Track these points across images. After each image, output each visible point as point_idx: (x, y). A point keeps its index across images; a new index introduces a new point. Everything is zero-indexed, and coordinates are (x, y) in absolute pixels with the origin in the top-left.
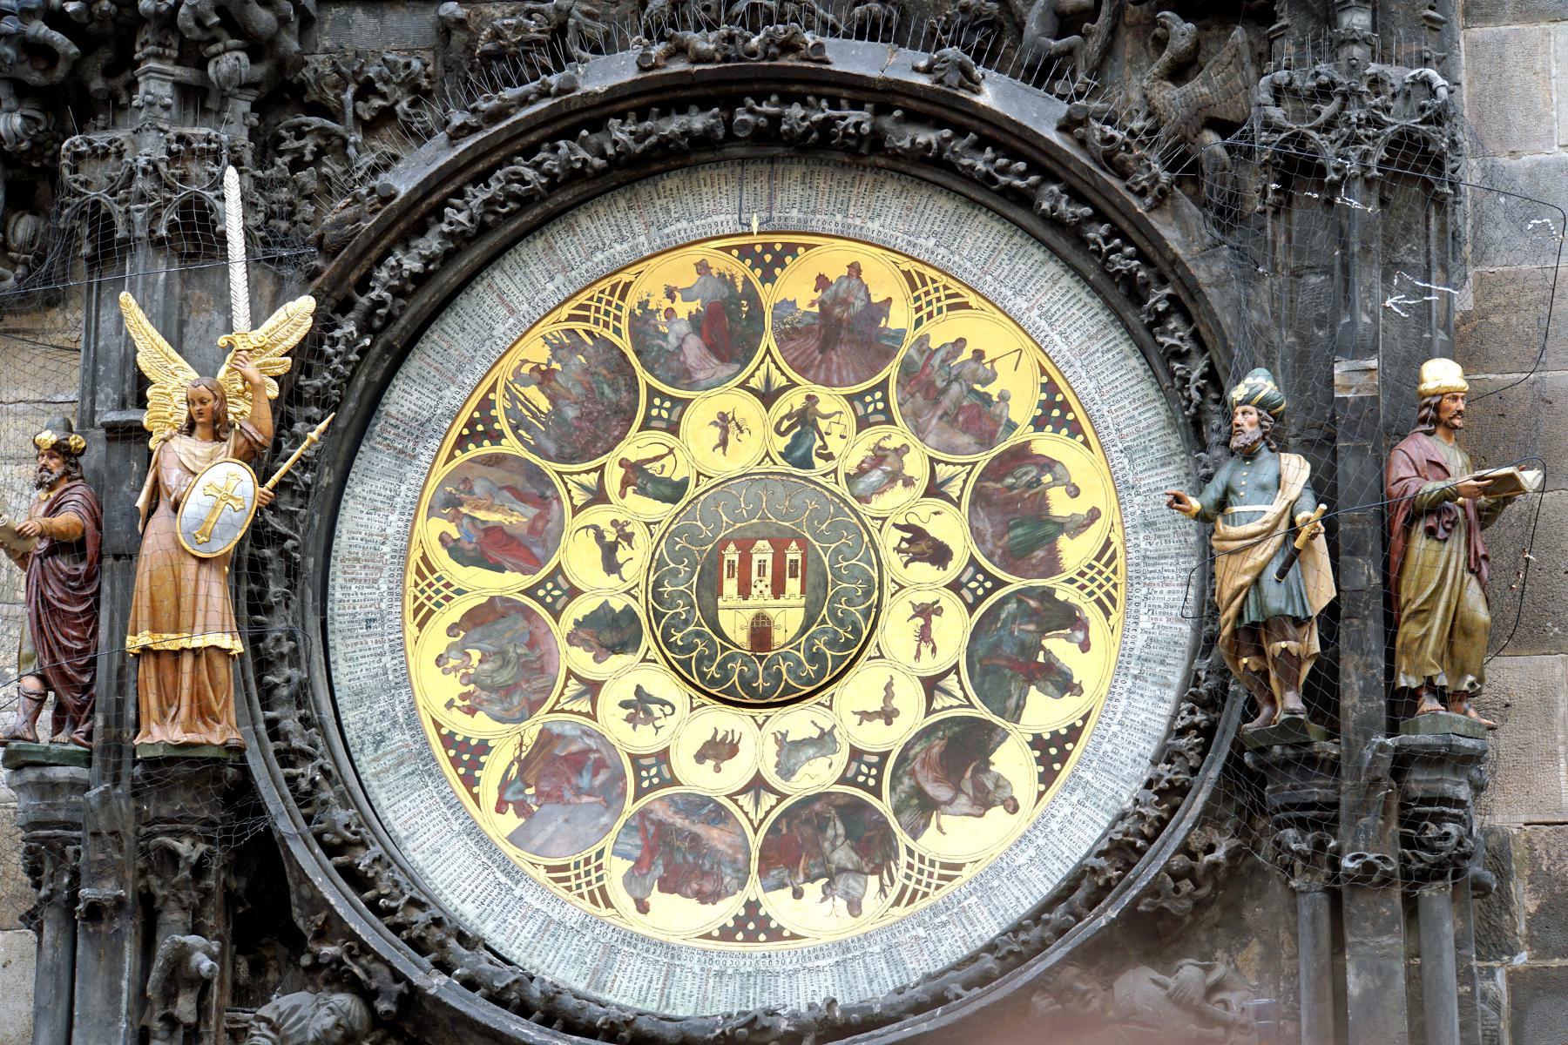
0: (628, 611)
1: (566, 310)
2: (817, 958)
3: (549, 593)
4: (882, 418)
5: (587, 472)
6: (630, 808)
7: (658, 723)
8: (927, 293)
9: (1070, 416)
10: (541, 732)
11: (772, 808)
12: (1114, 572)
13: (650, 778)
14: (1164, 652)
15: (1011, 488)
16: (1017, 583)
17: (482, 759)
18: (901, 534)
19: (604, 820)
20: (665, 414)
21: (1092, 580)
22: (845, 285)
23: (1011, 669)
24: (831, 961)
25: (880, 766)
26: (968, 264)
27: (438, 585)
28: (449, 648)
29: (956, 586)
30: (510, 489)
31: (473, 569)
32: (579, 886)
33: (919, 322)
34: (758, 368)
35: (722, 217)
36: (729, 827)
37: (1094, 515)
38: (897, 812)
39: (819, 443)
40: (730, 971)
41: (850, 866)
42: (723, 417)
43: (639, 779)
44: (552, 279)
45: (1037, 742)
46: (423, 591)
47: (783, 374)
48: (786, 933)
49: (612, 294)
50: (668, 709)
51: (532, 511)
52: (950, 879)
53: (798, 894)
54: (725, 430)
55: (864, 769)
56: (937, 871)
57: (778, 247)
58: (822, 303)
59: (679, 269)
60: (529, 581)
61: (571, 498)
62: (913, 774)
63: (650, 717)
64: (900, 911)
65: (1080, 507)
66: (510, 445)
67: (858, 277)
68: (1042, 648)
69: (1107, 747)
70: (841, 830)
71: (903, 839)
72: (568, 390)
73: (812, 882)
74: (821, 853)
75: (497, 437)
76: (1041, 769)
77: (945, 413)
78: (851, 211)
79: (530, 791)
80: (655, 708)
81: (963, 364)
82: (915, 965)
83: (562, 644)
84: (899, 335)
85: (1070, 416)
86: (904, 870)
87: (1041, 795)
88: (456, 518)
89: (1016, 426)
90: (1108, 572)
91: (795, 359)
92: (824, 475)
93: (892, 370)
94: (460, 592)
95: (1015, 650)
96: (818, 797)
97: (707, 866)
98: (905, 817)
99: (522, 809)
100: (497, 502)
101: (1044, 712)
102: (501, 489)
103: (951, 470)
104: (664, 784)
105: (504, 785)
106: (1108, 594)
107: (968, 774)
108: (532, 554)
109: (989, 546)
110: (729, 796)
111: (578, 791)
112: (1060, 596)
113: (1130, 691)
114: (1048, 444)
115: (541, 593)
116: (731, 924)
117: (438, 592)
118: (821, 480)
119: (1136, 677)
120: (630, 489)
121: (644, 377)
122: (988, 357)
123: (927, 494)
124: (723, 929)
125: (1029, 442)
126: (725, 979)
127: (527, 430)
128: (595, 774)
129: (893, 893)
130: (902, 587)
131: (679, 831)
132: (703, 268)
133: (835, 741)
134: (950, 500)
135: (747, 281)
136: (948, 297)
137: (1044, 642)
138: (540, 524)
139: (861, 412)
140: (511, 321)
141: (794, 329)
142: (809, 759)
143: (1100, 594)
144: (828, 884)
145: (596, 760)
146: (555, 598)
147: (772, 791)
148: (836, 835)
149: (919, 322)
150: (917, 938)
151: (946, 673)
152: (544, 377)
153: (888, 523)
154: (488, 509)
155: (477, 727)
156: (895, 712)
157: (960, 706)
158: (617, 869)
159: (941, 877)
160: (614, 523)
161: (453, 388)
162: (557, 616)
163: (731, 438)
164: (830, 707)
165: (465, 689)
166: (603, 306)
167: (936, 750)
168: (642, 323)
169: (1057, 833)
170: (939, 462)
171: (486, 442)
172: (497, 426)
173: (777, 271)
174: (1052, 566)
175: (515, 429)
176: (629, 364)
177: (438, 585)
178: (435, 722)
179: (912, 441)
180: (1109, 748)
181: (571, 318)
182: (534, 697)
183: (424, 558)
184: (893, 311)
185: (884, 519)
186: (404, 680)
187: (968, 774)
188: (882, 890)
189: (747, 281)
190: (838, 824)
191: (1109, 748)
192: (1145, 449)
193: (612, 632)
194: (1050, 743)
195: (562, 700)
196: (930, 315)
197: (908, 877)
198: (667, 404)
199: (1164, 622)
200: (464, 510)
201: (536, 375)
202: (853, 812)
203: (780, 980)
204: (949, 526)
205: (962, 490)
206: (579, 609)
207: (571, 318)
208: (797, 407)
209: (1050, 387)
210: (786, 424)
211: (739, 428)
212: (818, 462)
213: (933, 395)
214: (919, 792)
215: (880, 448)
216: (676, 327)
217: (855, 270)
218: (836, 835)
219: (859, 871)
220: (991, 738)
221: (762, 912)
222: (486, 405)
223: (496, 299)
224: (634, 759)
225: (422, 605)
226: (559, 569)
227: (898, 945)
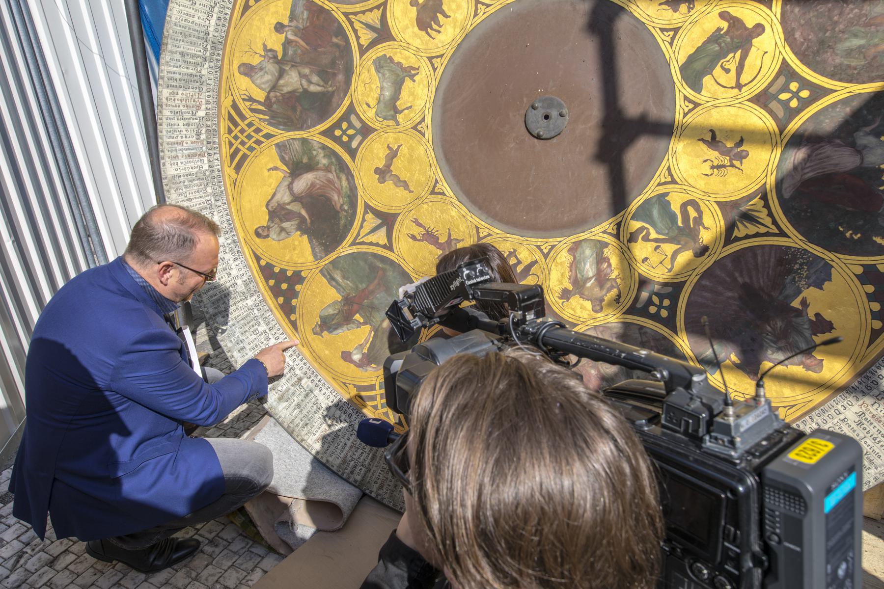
2: (219, 19)
11: (358, 38)
14: (305, 412)
23: (363, 290)
24: (211, 29)
25: (347, 147)
34: (770, 214)
38: (304, 141)
39: (653, 235)
41: (281, 82)
45: (297, 278)
47: (747, 237)
52: (233, 157)
53: (279, 28)
55: (351, 132)
56: (244, 150)
58: (799, 313)
62: (327, 169)
64: (227, 103)
68: (365, 323)
69: (262, 328)
70: (313, 88)
71: (283, 135)
73: (284, 45)
74: (304, 63)
82: (179, 96)
91: (755, 256)
95: (376, 302)
98: (297, 146)
101: (320, 295)
107: (304, 213)
119: (300, 379)
129: (243, 106)
137: (368, 328)
141: (790, 271)
142: (382, 88)
144: (275, 57)
147: (373, 44)
150: (199, 108)
153: (538, 256)
156: (382, 180)
157: (358, 234)
159: (237, 151)
164: (415, 128)
167: (336, 197)
185: (546, 256)
187: (304, 213)
188: (251, 99)
190: (319, 89)
194: (291, 288)
197: (250, 125)
198: (794, 104)
210: (693, 213)
211: (718, 167)
214: (310, 167)
218: (310, 82)
219: (274, 87)
220: (321, 244)
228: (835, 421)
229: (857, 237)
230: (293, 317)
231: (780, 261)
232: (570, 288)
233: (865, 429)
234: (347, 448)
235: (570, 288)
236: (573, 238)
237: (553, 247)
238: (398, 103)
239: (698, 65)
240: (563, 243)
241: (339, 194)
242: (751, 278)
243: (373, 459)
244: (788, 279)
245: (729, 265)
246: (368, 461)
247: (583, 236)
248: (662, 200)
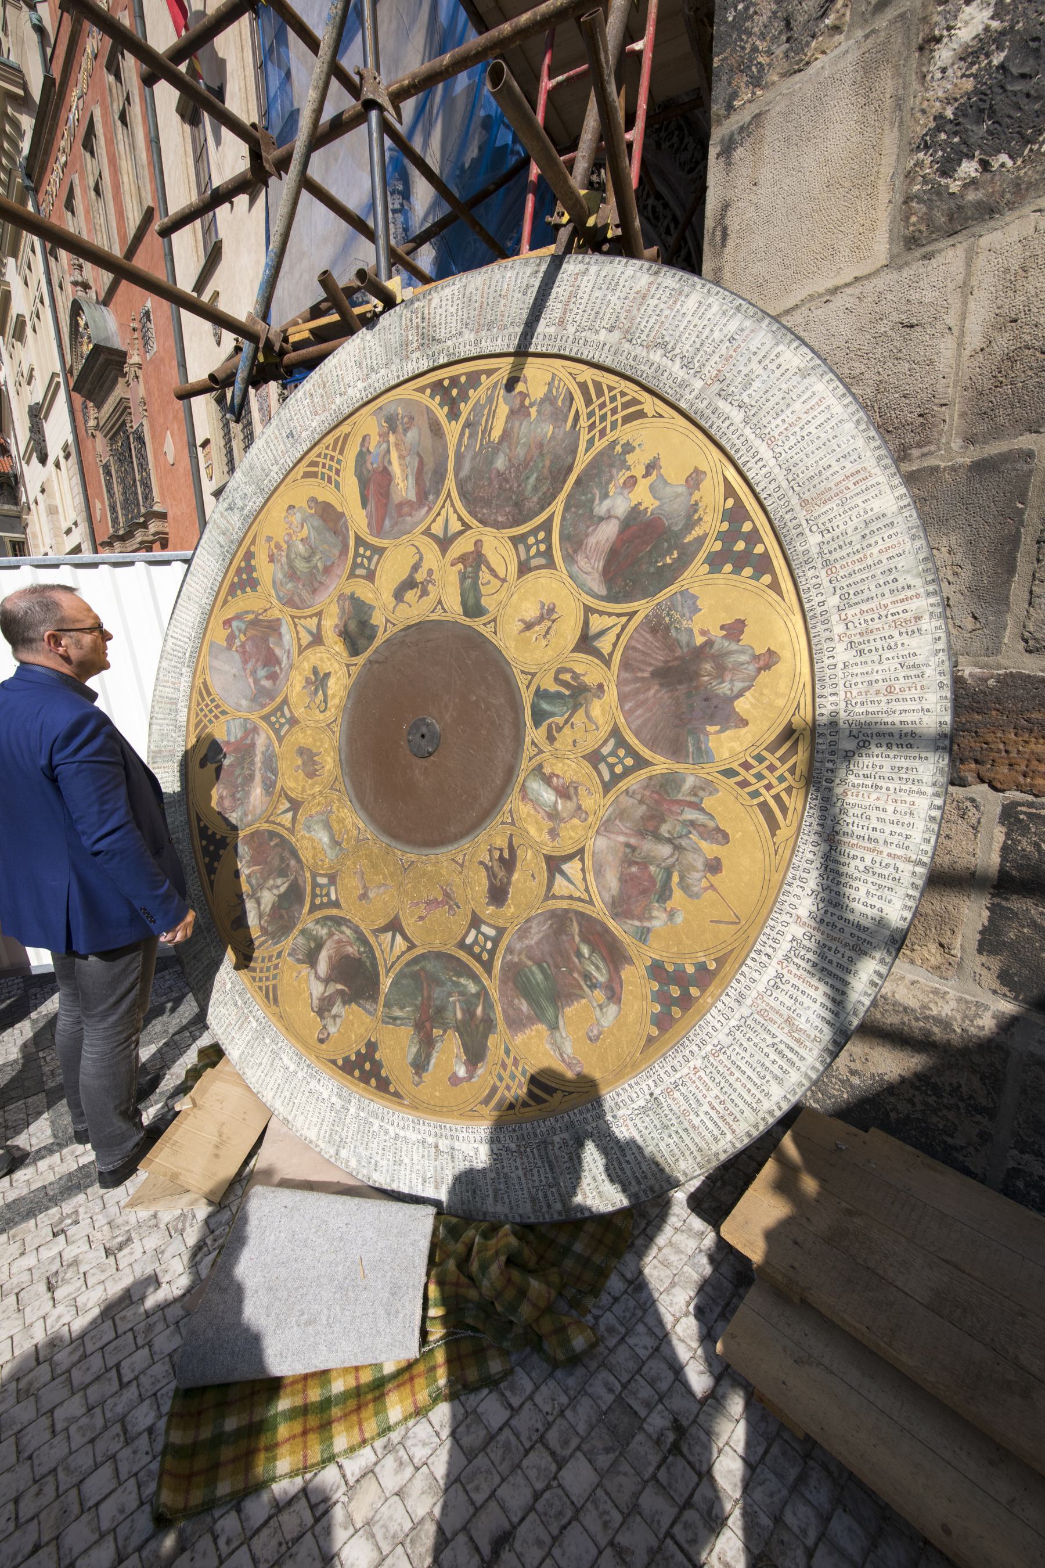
4: (607, 777)
6: (255, 717)
7: (312, 705)
8: (772, 768)
10: (279, 620)
15: (579, 954)
16: (493, 986)
18: (505, 845)
22: (744, 658)
23: (422, 1004)
29: (476, 922)
30: (421, 463)
32: (202, 710)
33: (729, 773)
39: (560, 720)
43: (273, 713)
45: (372, 1047)
47: (615, 645)
51: (412, 496)
52: (267, 997)
54: (541, 619)
56: (270, 983)
58: (709, 643)
62: (331, 935)
66: (452, 431)
67: (759, 670)
68: (445, 1032)
70: (282, 889)
72: (518, 443)
74: (266, 880)
75: (454, 415)
77: (634, 849)
78: (850, 612)
79: (243, 638)
81: (697, 850)
84: (703, 755)
88: (384, 436)
89: (644, 942)
91: (634, 649)
92: (533, 743)
95: (438, 1002)
96: (299, 861)
97: (238, 796)
98: (301, 940)
99: (231, 639)
100: (408, 459)
101: (397, 1048)
102: (418, 455)
105: (238, 617)
107: (339, 987)
108: (383, 520)
109: (518, 946)
110: (282, 789)
111: (254, 672)
112: (492, 1040)
119: (436, 1147)
120: (460, 566)
121: (558, 506)
122: (715, 879)
123: (549, 859)
124: (206, 828)
127: (469, 437)
128: (267, 678)
131: (252, 763)
132: (695, 479)
135: (700, 540)
138: (406, 509)
139: (605, 750)
141: (667, 628)
148: (278, 887)
149: (729, 773)
154: (401, 457)
155: (266, 571)
160: (430, 572)
162: (352, 575)
167: (350, 949)
170: (582, 860)
174: (516, 1024)
175: (468, 424)
176: (564, 481)
180: (376, 1128)
181: (583, 387)
182: (296, 599)
185: (513, 823)
187: (339, 987)
189: (700, 540)
191: (376, 1128)
192: (666, 1127)
196: (744, 784)
198: (543, 547)
200: (392, 438)
207: (583, 387)
210: (567, 677)
211: (547, 632)
213: (649, 826)
214: (319, 947)
215: (576, 788)
217: (768, 660)
218: (278, 887)
220: (367, 999)
224: (285, 701)
226: (380, 551)
228: (841, 675)
229: (675, 555)
231: (654, 631)
232: (551, 824)
233: (870, 651)
234: (523, 1181)
235: (551, 824)
236: (517, 788)
237: (510, 811)
239: (471, 601)
240: (513, 802)
241: (350, 944)
242: (651, 664)
243: (551, 1169)
244: (673, 633)
245: (627, 675)
246: (549, 1175)
247: (521, 779)
248: (541, 694)
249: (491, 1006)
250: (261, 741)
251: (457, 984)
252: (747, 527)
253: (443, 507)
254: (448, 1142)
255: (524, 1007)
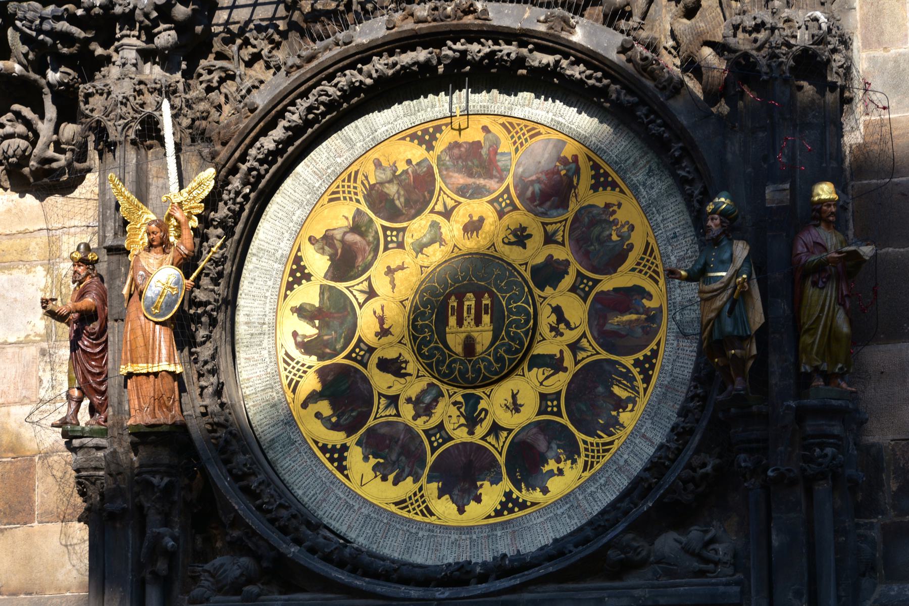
0: (542, 289)
1: (615, 447)
3: (586, 285)
5: (583, 359)
6: (509, 180)
9: (328, 455)
10: (568, 207)
11: (436, 204)
12: (287, 377)
13: (504, 200)
14: (252, 340)
15: (352, 411)
17: (593, 181)
19: (521, 170)
20: (549, 403)
21: (298, 370)
24: (379, 131)
26: (398, 526)
27: (645, 270)
28: (629, 236)
30: (623, 336)
31: (630, 285)
32: (521, 129)
33: (421, 489)
34: (504, 442)
35: (539, 521)
36: (455, 186)
37: (305, 405)
38: (371, 220)
39: (462, 410)
40: (429, 109)
41: (387, 185)
42: (517, 410)
44: (626, 461)
45: (308, 277)
46: (652, 263)
47: (490, 443)
48: (408, 139)
49: (592, 463)
50: (506, 241)
51: (608, 327)
53: (409, 162)
55: (394, 239)
56: (341, 195)
57: (505, 513)
59: (557, 487)
60: (599, 288)
61: (588, 341)
62: (369, 243)
63: (514, 233)
64: (353, 168)
65: (313, 408)
66: (628, 361)
68: (317, 328)
70: (397, 202)
71: (364, 208)
73: (403, 171)
74: (404, 188)
76: (302, 264)
77: (397, 442)
78: (468, 542)
79: (563, 172)
80: (513, 239)
82: (337, 142)
83: (571, 259)
85: (328, 455)
86: (359, 190)
87: (299, 250)
88: (647, 311)
90: (291, 376)
92: (455, 393)
93: (431, 459)
94: (633, 270)
95: (331, 323)
96: (414, 217)
97: (460, 162)
98: (366, 219)
100: (628, 327)
101: (309, 294)
103: (387, 413)
104: (496, 200)
105: (577, 171)
106: (289, 364)
107: (340, 251)
109: (358, 376)
110: (460, 203)
111: (538, 181)
112: (314, 358)
113: (265, 315)
114: (336, 438)
115: (590, 283)
116: (438, 135)
117: (645, 266)
118: (456, 390)
119: (264, 324)
121: (565, 420)
122: (379, 479)
125: (348, 437)
126: (430, 105)
128: (533, 193)
129: (360, 176)
130: (400, 342)
131: (480, 176)
132: (545, 491)
133: (414, 249)
134: (384, 396)
135: (520, 490)
136: (407, 507)
137: (317, 331)
139: (443, 433)
140: (643, 431)
141: (489, 470)
143: (293, 364)
144: (395, 172)
145: (535, 201)
146: (582, 283)
147: (439, 213)
149: (421, 489)
150: (340, 156)
151: (365, 302)
152: (621, 404)
154: (631, 321)
155: (600, 199)
156: (387, 274)
158: (506, 145)
160: (562, 335)
161: (666, 383)
162: (579, 273)
163: (510, 400)
165: (614, 216)
166: (596, 454)
167: (360, 259)
168: (572, 451)
169: (284, 232)
170: (395, 415)
171: (642, 358)
172: (638, 369)
173: (504, 499)
175: (629, 371)
177: (645, 270)
178: (624, 193)
179: (412, 424)
181: (612, 443)
182: (576, 225)
183: (657, 282)
184: (436, 493)
185: (418, 377)
186: (646, 210)
187: (340, 251)
188: (366, 177)
193: (548, 274)
194: (301, 279)
195: (562, 228)
197: (355, 188)
199: (256, 356)
200: (643, 316)
201: (624, 405)
202: (393, 214)
203: (402, 113)
204: (381, 382)
205: (379, 403)
206: (568, 281)
207: (612, 443)
208: (478, 427)
209: (342, 469)
210: (482, 415)
211: (507, 407)
212: (460, 399)
214: (363, 234)
216: (554, 454)
217: (461, 511)
218: (399, 199)
219: (381, 184)
220: (333, 273)
221: (424, 146)
222: (647, 380)
223: (654, 441)
225: (650, 255)
227: (349, 150)
230: (288, 292)
238: (425, 249)
240: (428, 379)
241: (363, 260)
249: (330, 358)
250: (491, 184)
251: (340, 337)
252: (516, 509)
253: (593, 348)
254: (267, 332)
255: (329, 378)
